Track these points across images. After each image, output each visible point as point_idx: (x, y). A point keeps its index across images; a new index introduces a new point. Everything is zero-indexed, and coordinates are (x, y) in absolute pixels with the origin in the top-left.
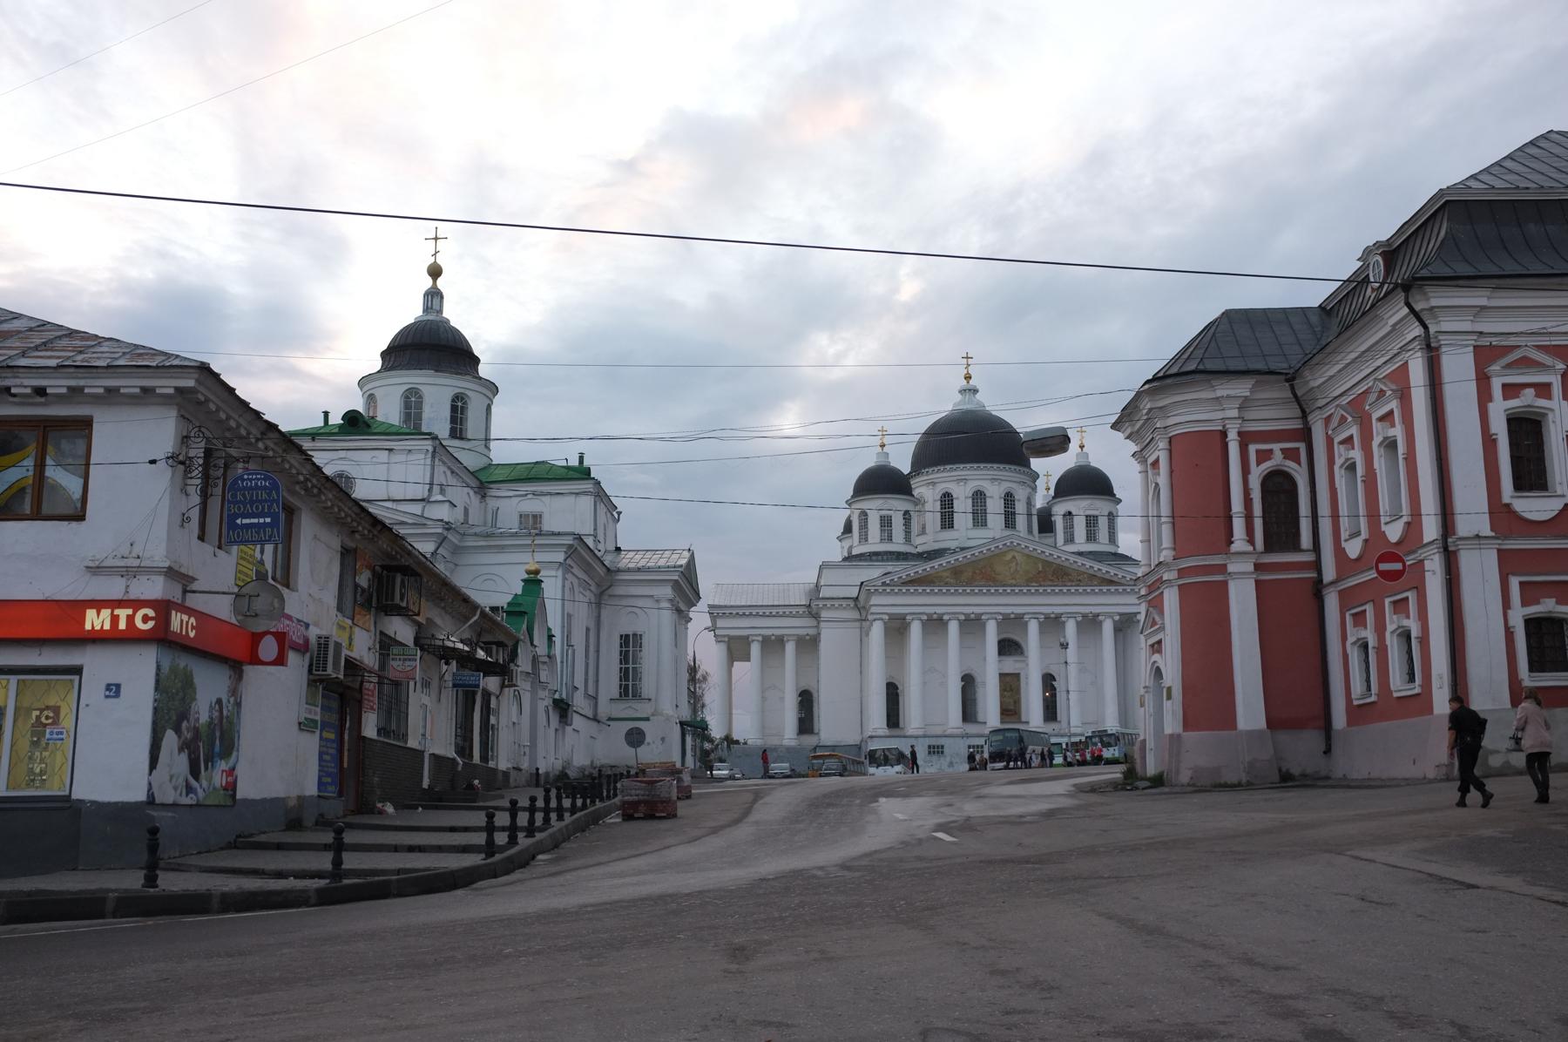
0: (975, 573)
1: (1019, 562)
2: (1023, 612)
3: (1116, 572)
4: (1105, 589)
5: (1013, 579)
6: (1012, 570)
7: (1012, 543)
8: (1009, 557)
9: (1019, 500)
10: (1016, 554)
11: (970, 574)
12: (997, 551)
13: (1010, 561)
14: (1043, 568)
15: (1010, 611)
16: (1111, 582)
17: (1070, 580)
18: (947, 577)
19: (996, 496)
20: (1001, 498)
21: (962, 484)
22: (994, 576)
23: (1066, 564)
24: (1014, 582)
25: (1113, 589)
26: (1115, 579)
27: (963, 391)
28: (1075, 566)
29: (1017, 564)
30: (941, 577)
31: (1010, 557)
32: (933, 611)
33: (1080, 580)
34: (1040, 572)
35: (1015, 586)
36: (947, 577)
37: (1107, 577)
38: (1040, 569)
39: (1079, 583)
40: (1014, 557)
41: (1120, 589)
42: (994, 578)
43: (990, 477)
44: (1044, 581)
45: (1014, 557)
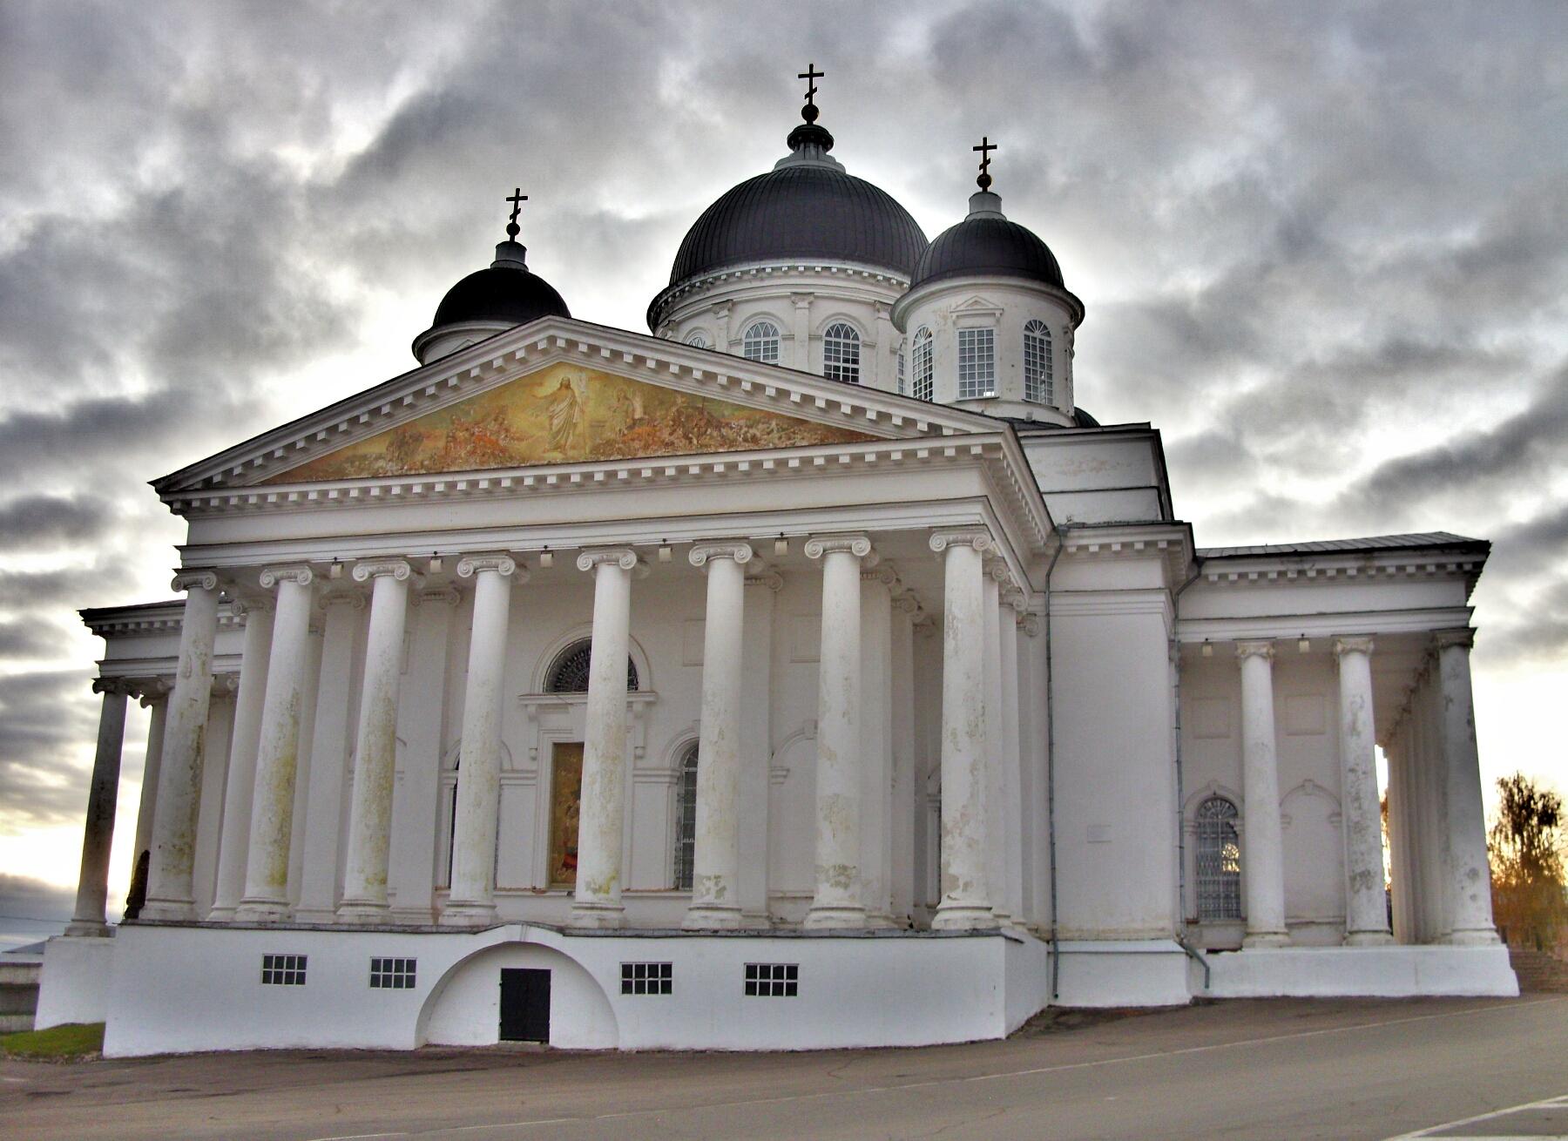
0: (454, 438)
1: (579, 400)
2: (575, 544)
3: (857, 403)
4: (819, 455)
5: (557, 447)
6: (555, 422)
7: (552, 340)
8: (551, 385)
9: (872, 346)
10: (574, 377)
11: (441, 444)
12: (515, 372)
13: (553, 399)
14: (645, 413)
15: (537, 546)
16: (852, 437)
17: (725, 441)
18: (379, 457)
19: (802, 333)
20: (813, 338)
21: (725, 312)
22: (502, 443)
23: (712, 392)
24: (557, 456)
25: (844, 453)
26: (859, 426)
27: (796, 139)
28: (736, 397)
29: (572, 404)
30: (365, 457)
31: (559, 386)
32: (329, 557)
33: (754, 439)
34: (635, 422)
35: (550, 465)
36: (379, 457)
37: (834, 421)
38: (637, 417)
39: (755, 445)
40: (566, 386)
41: (870, 452)
42: (503, 450)
43: (788, 291)
44: (646, 447)
45: (566, 386)
